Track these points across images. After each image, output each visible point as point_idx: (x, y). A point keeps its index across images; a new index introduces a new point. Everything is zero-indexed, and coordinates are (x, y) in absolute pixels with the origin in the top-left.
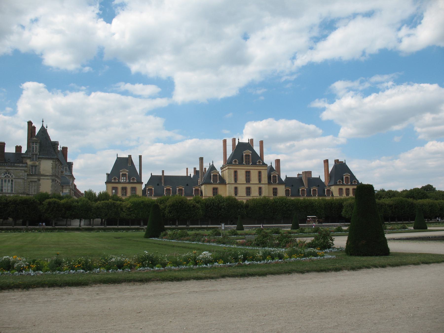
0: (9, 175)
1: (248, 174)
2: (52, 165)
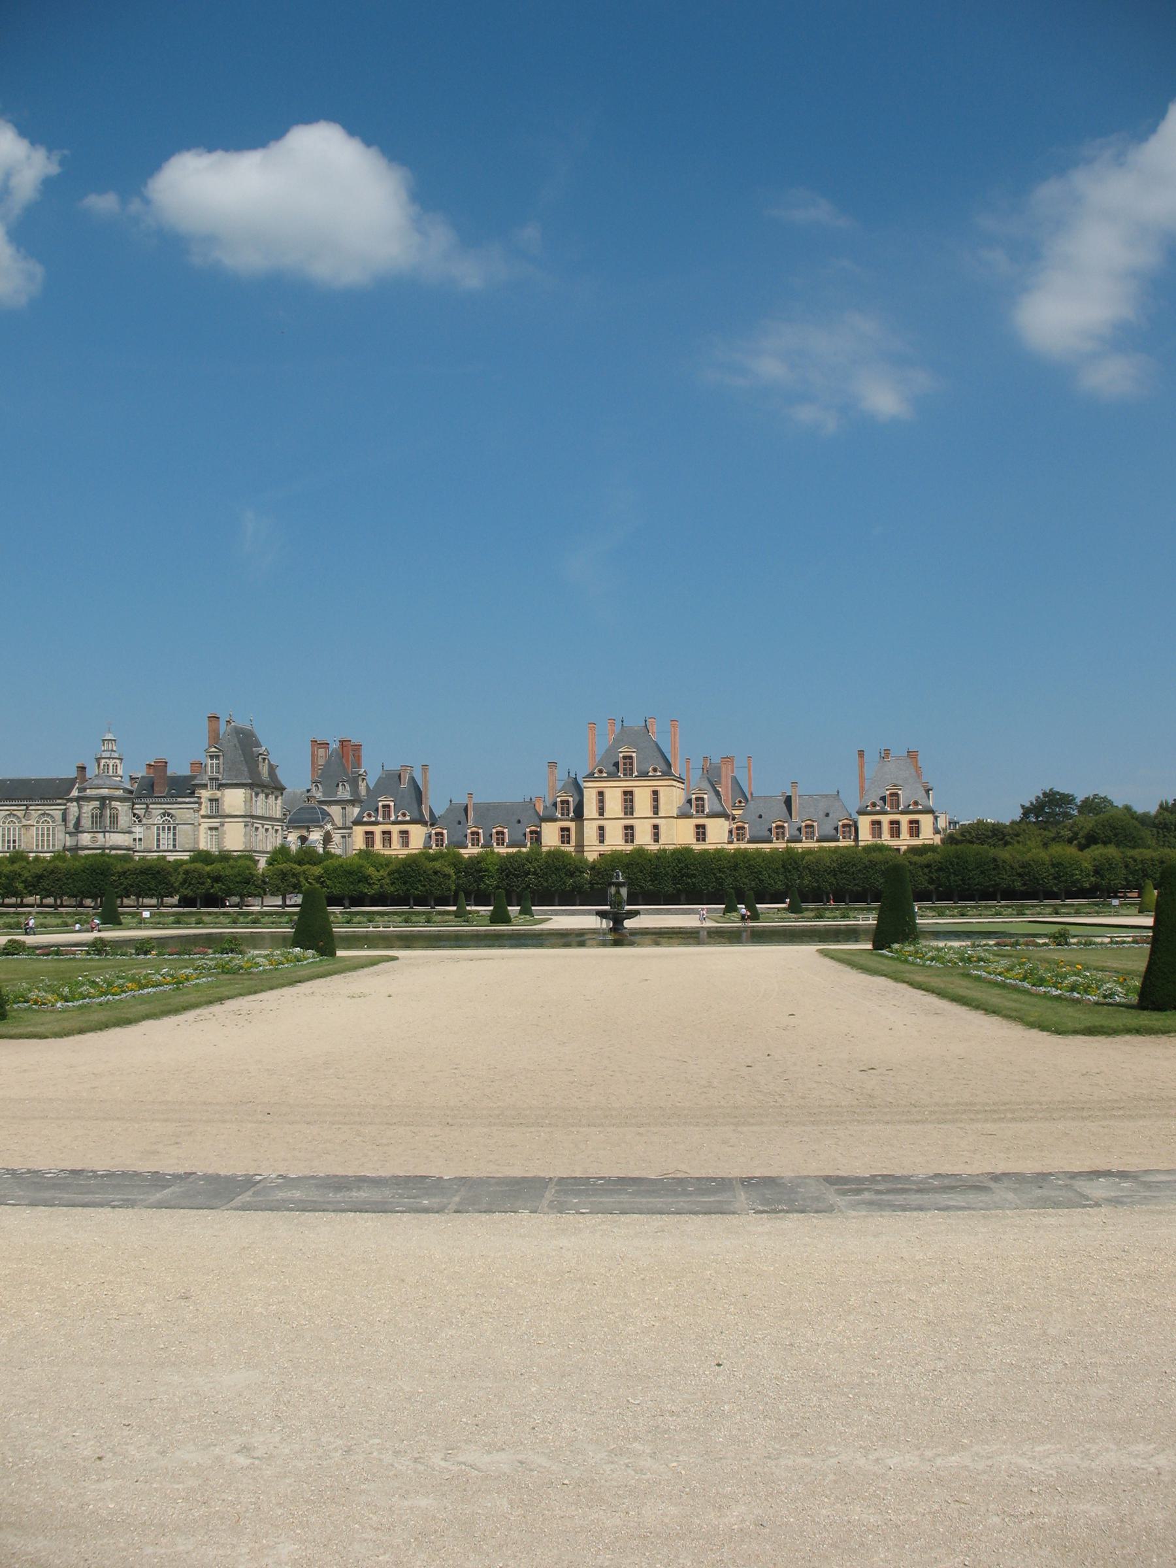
0: (169, 818)
1: (628, 795)
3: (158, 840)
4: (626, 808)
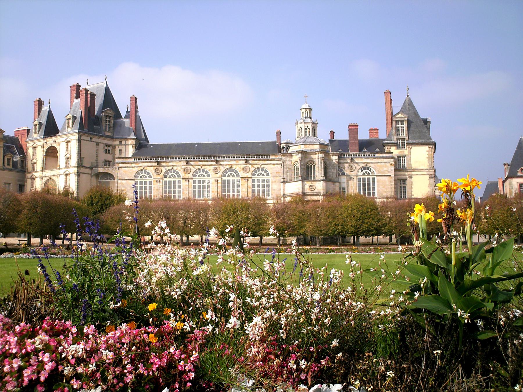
2: (427, 153)
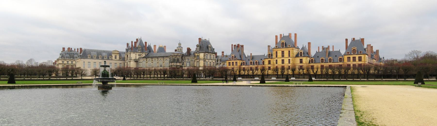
1: (283, 52)
3: (187, 64)
4: (282, 55)
